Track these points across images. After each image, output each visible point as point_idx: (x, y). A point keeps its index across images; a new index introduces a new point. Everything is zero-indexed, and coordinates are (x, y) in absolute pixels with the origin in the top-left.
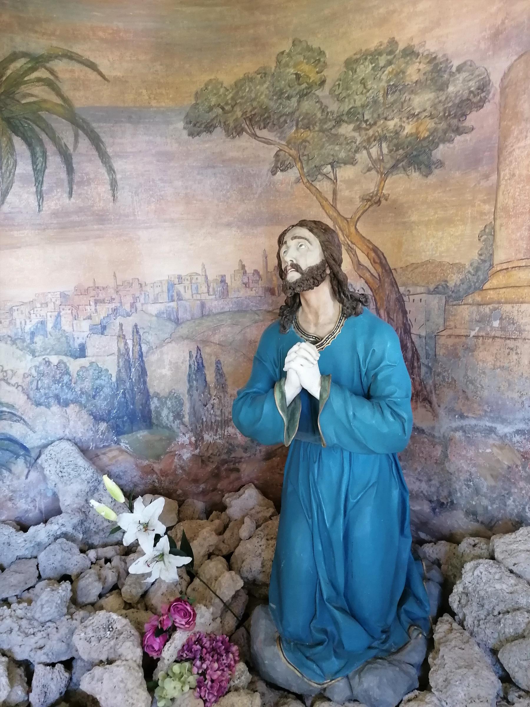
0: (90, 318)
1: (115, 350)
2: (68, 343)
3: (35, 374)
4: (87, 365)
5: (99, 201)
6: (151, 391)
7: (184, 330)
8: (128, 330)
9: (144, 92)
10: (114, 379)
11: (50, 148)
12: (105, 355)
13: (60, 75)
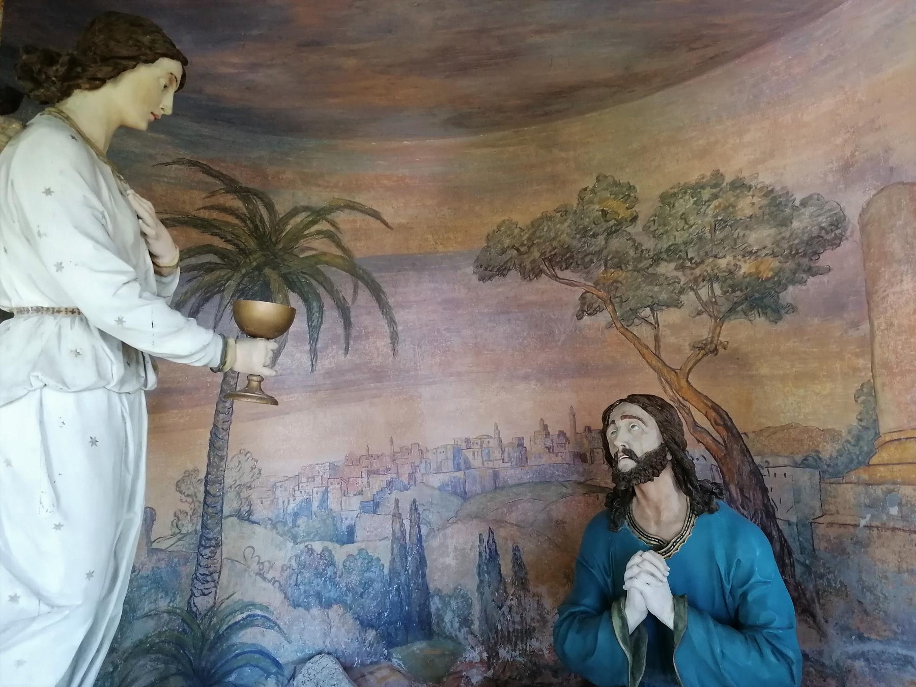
0: (361, 493)
1: (389, 533)
2: (335, 525)
3: (295, 565)
4: (355, 553)
5: (378, 356)
6: (432, 587)
7: (472, 507)
8: (405, 506)
9: (430, 237)
10: (386, 571)
11: (327, 301)
12: (377, 539)
13: (342, 226)
